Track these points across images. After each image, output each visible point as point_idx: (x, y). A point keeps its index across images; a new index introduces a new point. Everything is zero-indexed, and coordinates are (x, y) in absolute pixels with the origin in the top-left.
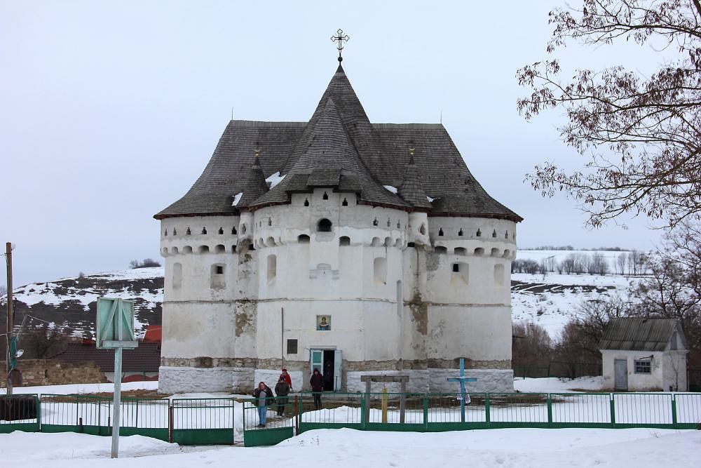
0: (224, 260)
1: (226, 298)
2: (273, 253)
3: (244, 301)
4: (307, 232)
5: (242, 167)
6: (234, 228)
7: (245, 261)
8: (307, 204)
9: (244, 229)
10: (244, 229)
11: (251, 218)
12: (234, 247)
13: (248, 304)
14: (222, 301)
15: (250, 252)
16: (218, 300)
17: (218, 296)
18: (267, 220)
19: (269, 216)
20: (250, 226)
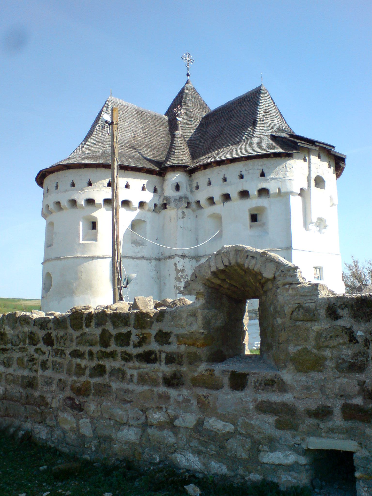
0: (144, 217)
1: (146, 255)
2: (261, 205)
3: (183, 256)
4: (305, 186)
5: (134, 137)
6: (155, 186)
7: (183, 218)
8: (305, 160)
9: (177, 188)
10: (177, 188)
11: (188, 177)
12: (155, 205)
13: (186, 260)
14: (142, 258)
15: (185, 210)
16: (139, 255)
17: (138, 252)
18: (259, 172)
19: (260, 168)
20: (185, 185)
